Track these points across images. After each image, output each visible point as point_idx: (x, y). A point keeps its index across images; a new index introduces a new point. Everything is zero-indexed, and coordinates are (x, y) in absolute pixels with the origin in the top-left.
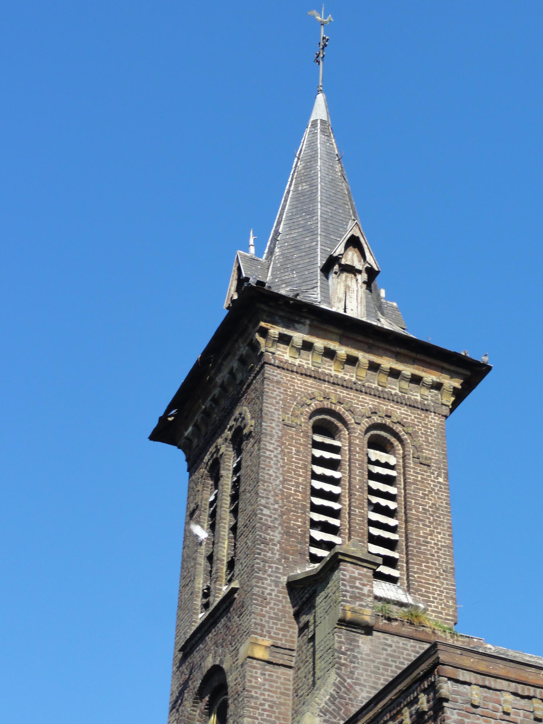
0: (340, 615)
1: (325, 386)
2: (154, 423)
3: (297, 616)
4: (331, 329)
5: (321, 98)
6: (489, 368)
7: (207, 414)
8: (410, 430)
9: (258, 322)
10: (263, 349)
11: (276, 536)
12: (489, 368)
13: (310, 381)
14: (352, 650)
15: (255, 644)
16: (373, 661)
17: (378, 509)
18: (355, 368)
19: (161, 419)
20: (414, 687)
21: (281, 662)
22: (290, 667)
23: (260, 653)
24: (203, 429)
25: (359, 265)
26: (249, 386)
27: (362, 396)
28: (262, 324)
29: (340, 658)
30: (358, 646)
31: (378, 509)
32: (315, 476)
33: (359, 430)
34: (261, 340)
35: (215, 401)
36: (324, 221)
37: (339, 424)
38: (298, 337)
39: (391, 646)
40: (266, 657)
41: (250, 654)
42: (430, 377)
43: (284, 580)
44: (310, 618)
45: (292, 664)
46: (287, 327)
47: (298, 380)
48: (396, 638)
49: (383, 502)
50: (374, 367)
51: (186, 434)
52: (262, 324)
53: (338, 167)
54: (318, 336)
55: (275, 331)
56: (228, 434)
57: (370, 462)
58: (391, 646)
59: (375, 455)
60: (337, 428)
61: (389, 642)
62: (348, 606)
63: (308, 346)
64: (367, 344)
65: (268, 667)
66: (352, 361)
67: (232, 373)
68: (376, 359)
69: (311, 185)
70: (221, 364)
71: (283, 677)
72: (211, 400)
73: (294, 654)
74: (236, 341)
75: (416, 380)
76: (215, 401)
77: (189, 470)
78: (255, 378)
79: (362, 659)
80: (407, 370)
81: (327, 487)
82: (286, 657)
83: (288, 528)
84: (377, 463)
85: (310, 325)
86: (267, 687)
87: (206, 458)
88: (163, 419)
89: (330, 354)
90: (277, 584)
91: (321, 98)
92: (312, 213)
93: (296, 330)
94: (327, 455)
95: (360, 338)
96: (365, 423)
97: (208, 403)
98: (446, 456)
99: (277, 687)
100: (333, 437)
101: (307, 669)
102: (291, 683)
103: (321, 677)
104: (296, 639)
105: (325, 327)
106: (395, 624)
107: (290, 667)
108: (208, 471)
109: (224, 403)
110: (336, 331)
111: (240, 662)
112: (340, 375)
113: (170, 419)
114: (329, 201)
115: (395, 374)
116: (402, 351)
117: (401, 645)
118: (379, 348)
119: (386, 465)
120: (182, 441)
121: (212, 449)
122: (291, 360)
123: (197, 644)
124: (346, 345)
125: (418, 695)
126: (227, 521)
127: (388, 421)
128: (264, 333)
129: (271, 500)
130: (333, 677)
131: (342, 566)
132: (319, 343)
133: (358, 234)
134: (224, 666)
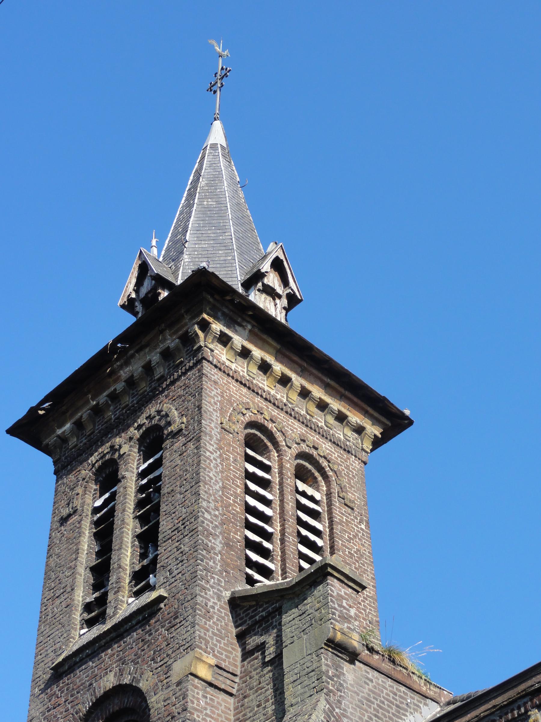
0: (331, 635)
1: (258, 399)
2: (20, 413)
3: (241, 637)
4: (270, 340)
5: (217, 126)
6: (410, 423)
7: (97, 411)
8: (335, 468)
9: (201, 313)
10: (202, 343)
11: (218, 544)
12: (410, 423)
13: (245, 390)
14: (338, 677)
15: (200, 660)
16: (358, 695)
17: (305, 541)
18: (285, 390)
19: (32, 408)
20: (520, 702)
21: (223, 686)
22: (231, 695)
23: (203, 672)
24: (89, 428)
25: (279, 289)
26: (173, 383)
27: (292, 420)
28: (205, 316)
29: (328, 683)
30: (344, 674)
31: (305, 541)
32: (248, 491)
33: (289, 454)
34: (201, 334)
35: (114, 397)
36: (237, 239)
37: (269, 444)
38: (238, 341)
39: (372, 681)
40: (209, 678)
41: (193, 670)
42: (355, 418)
43: (227, 595)
44: (270, 639)
45: (234, 691)
46: (228, 327)
47: (234, 386)
48: (376, 674)
49: (312, 537)
50: (304, 394)
51: (59, 432)
52: (205, 316)
53: (241, 194)
54: (256, 345)
55: (217, 327)
56: (134, 432)
57: (297, 491)
58: (372, 681)
59: (302, 486)
60: (267, 447)
61: (370, 676)
62: (338, 626)
63: (245, 353)
64: (300, 366)
65: (209, 689)
66: (284, 381)
67: (148, 368)
68: (309, 386)
69: (218, 203)
70: (133, 356)
71: (223, 704)
72: (108, 396)
73: (237, 680)
74: (162, 332)
75: (341, 418)
76: (114, 397)
77: (56, 473)
78: (184, 374)
79: (347, 688)
80: (335, 405)
81: (261, 507)
82: (228, 682)
83: (228, 539)
84: (304, 494)
85: (250, 331)
86: (208, 712)
87: (93, 459)
88: (33, 411)
89: (265, 367)
90: (219, 598)
91: (217, 126)
92: (224, 229)
93: (236, 332)
94: (260, 473)
95: (296, 358)
96: (295, 450)
97: (103, 398)
98: (366, 504)
99: (218, 715)
100: (261, 454)
101: (262, 697)
102: (232, 713)
103: (297, 703)
104: (239, 664)
105: (265, 337)
106: (376, 657)
107: (231, 695)
108: (95, 474)
109: (127, 400)
110: (274, 344)
111: (174, 679)
112: (273, 392)
113: (41, 412)
114: (239, 221)
115: (322, 406)
116: (332, 383)
117: (380, 682)
118: (311, 374)
119: (311, 499)
120: (51, 440)
121: (105, 448)
122: (228, 363)
123: (83, 661)
124: (281, 362)
125: (526, 711)
126: (131, 527)
127: (315, 453)
128: (205, 326)
129: (212, 505)
130: (323, 704)
131: (330, 580)
132: (257, 353)
133: (282, 257)
134: (142, 685)
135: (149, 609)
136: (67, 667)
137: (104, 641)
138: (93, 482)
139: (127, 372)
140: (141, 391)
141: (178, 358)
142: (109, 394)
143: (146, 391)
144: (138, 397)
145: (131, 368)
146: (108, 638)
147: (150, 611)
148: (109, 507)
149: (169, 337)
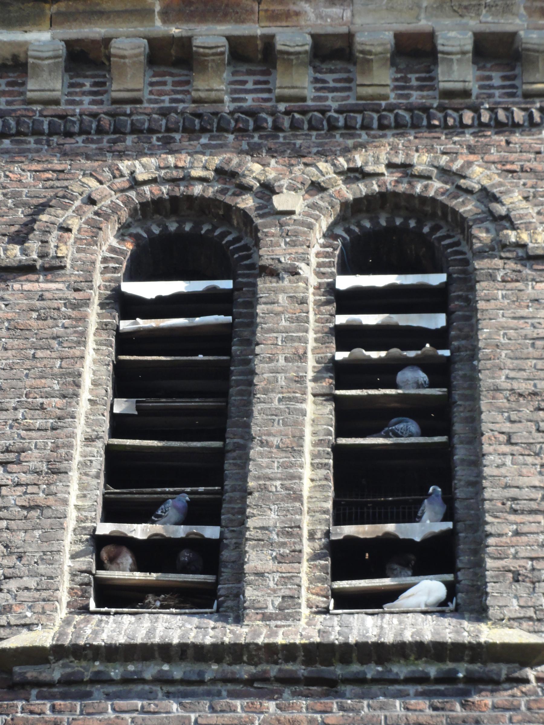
108: (133, 213)
135: (472, 661)
136: (57, 675)
137: (252, 669)
138: (117, 226)
139: (328, 16)
140: (370, 91)
141: (538, 77)
142: (239, 37)
143: (385, 97)
144: (348, 97)
145: (347, 14)
146: (273, 670)
147: (476, 667)
148: (198, 320)
149: (522, 11)
